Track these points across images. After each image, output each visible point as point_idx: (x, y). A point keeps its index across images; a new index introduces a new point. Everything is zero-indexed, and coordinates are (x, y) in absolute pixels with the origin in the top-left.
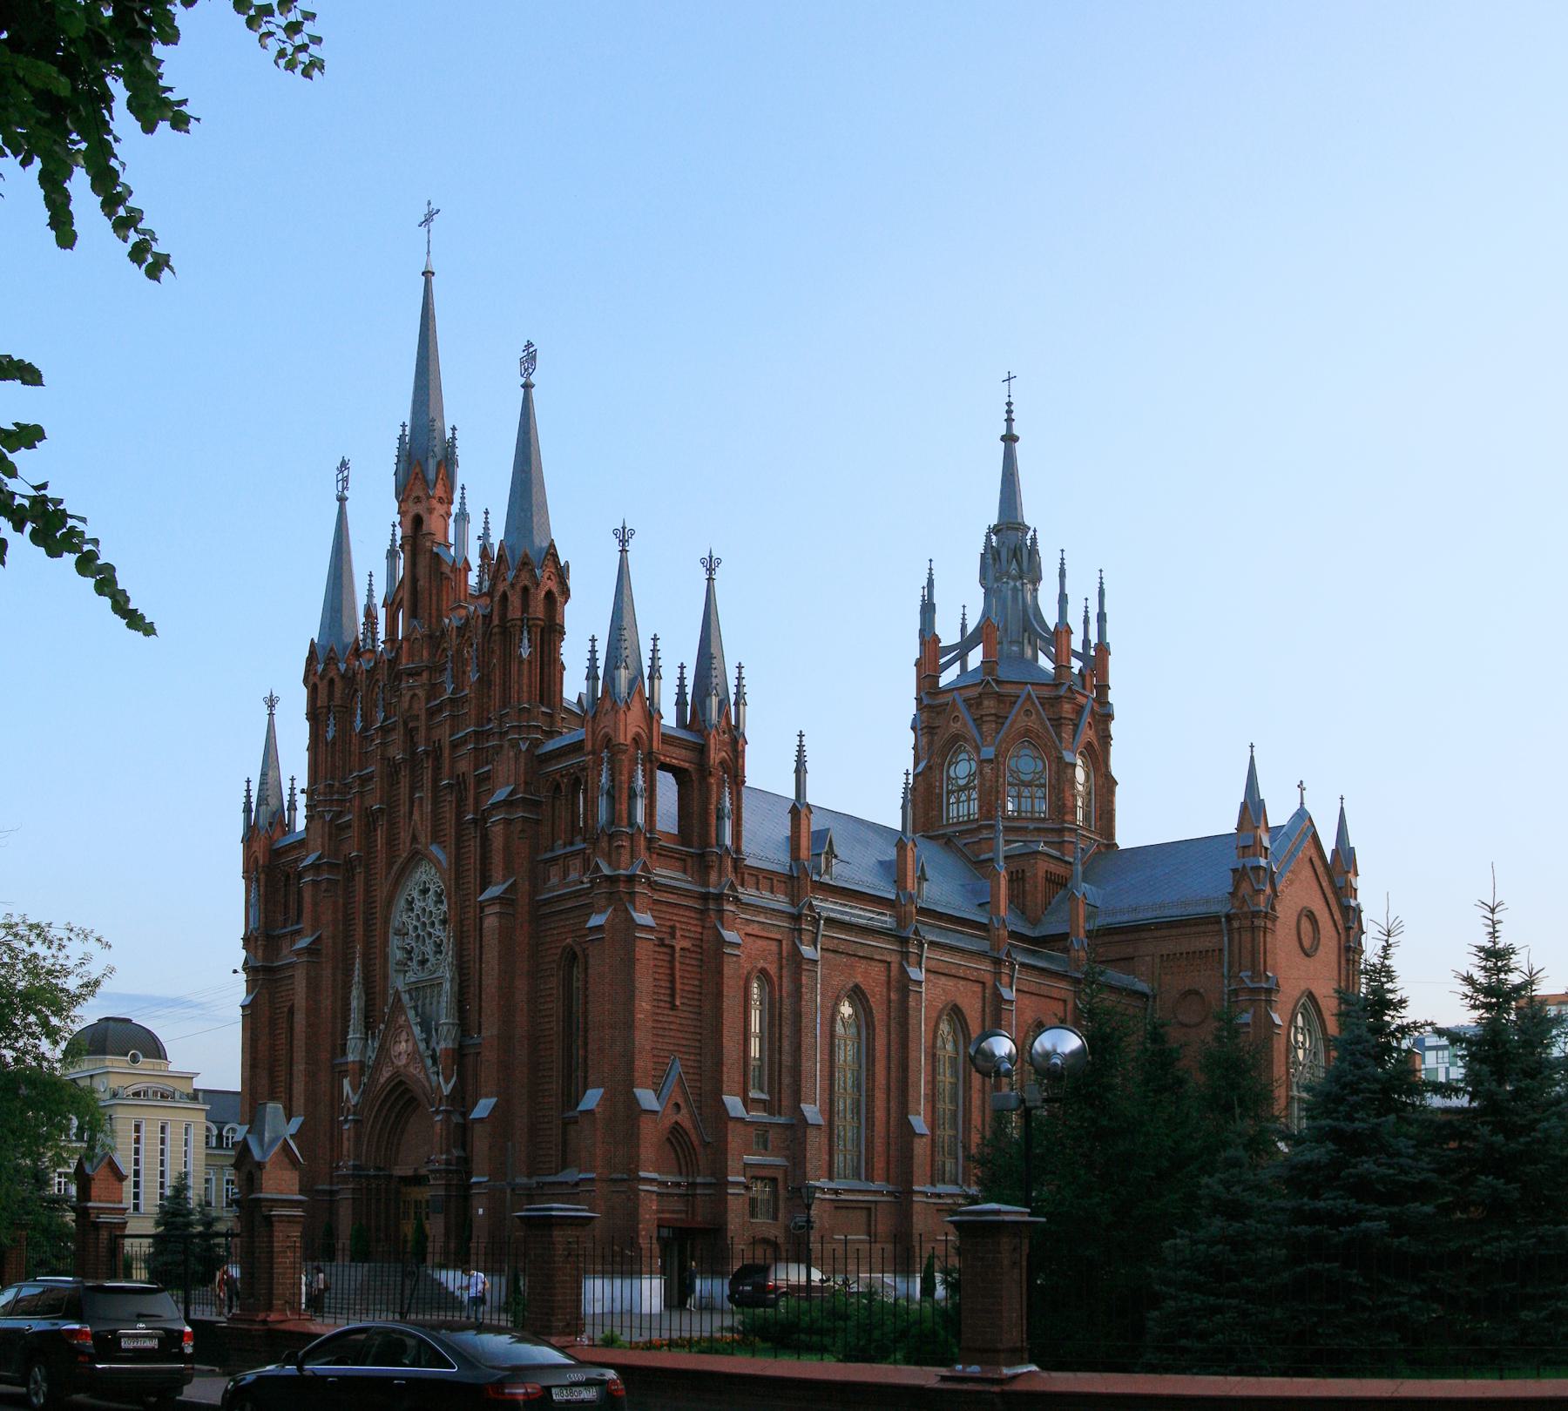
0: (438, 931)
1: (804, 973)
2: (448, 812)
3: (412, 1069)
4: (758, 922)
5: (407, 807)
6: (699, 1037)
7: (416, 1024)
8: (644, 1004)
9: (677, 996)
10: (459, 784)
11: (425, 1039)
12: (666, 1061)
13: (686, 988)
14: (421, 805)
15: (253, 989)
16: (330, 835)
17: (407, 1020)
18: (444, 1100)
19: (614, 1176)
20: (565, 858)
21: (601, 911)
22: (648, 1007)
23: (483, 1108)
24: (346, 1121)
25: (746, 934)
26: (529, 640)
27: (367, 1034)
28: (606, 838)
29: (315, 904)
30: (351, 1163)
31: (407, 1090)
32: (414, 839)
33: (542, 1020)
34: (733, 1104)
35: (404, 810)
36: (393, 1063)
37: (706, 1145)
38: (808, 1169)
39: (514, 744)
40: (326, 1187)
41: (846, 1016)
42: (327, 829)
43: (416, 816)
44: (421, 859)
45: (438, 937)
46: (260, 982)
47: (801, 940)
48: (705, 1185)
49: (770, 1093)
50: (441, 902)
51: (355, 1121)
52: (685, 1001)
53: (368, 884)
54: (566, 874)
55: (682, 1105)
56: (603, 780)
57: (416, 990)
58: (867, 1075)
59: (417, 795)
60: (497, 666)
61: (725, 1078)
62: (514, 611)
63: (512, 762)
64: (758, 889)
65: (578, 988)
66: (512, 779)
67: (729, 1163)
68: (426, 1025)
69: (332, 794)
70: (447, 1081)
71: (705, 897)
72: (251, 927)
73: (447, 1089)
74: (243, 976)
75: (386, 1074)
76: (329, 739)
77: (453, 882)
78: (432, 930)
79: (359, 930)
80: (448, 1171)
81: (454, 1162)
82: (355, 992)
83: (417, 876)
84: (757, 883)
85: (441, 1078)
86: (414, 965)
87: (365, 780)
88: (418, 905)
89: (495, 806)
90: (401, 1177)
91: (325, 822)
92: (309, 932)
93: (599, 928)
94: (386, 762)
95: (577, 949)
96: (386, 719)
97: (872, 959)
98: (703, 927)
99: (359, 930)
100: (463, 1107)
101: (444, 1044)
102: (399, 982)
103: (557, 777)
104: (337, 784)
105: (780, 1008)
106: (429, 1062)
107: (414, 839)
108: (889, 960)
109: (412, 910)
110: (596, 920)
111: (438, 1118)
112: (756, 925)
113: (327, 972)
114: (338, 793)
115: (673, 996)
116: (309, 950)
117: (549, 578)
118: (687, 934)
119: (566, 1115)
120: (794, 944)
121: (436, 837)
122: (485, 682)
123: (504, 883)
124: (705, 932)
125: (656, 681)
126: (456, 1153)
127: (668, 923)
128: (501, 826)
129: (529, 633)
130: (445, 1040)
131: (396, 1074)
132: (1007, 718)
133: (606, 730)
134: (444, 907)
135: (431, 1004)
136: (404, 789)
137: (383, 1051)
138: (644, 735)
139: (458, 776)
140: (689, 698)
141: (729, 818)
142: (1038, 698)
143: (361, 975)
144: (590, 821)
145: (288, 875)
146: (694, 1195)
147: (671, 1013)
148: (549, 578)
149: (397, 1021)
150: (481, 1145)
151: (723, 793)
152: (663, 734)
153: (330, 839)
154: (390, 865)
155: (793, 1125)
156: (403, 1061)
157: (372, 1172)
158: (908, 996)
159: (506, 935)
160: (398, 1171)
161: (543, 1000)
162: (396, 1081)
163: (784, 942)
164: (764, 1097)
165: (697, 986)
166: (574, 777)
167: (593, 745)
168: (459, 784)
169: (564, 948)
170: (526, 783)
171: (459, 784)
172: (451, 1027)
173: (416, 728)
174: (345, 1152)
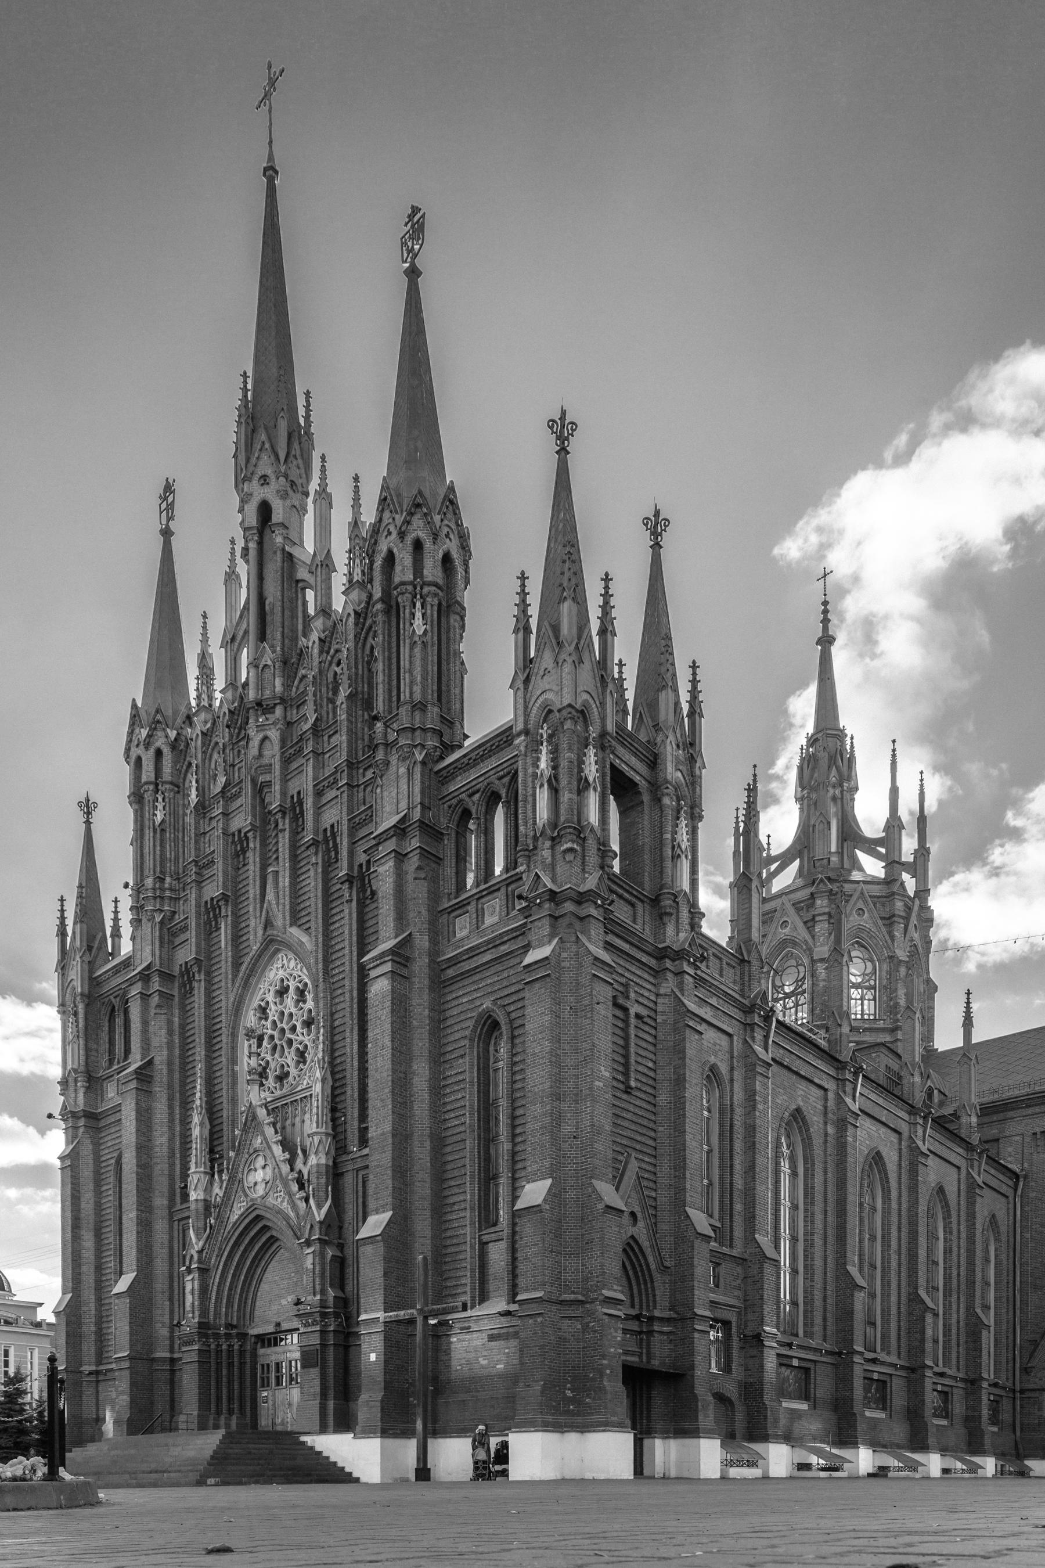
1: (759, 1078)
2: (312, 882)
5: (258, 887)
8: (602, 1068)
19: (566, 1297)
20: (478, 899)
32: (268, 924)
35: (253, 891)
38: (765, 1313)
43: (270, 896)
67: (696, 1292)
89: (381, 839)
97: (811, 1082)
107: (268, 924)
121: (295, 919)
123: (396, 937)
158: (846, 1130)
159: (400, 1004)
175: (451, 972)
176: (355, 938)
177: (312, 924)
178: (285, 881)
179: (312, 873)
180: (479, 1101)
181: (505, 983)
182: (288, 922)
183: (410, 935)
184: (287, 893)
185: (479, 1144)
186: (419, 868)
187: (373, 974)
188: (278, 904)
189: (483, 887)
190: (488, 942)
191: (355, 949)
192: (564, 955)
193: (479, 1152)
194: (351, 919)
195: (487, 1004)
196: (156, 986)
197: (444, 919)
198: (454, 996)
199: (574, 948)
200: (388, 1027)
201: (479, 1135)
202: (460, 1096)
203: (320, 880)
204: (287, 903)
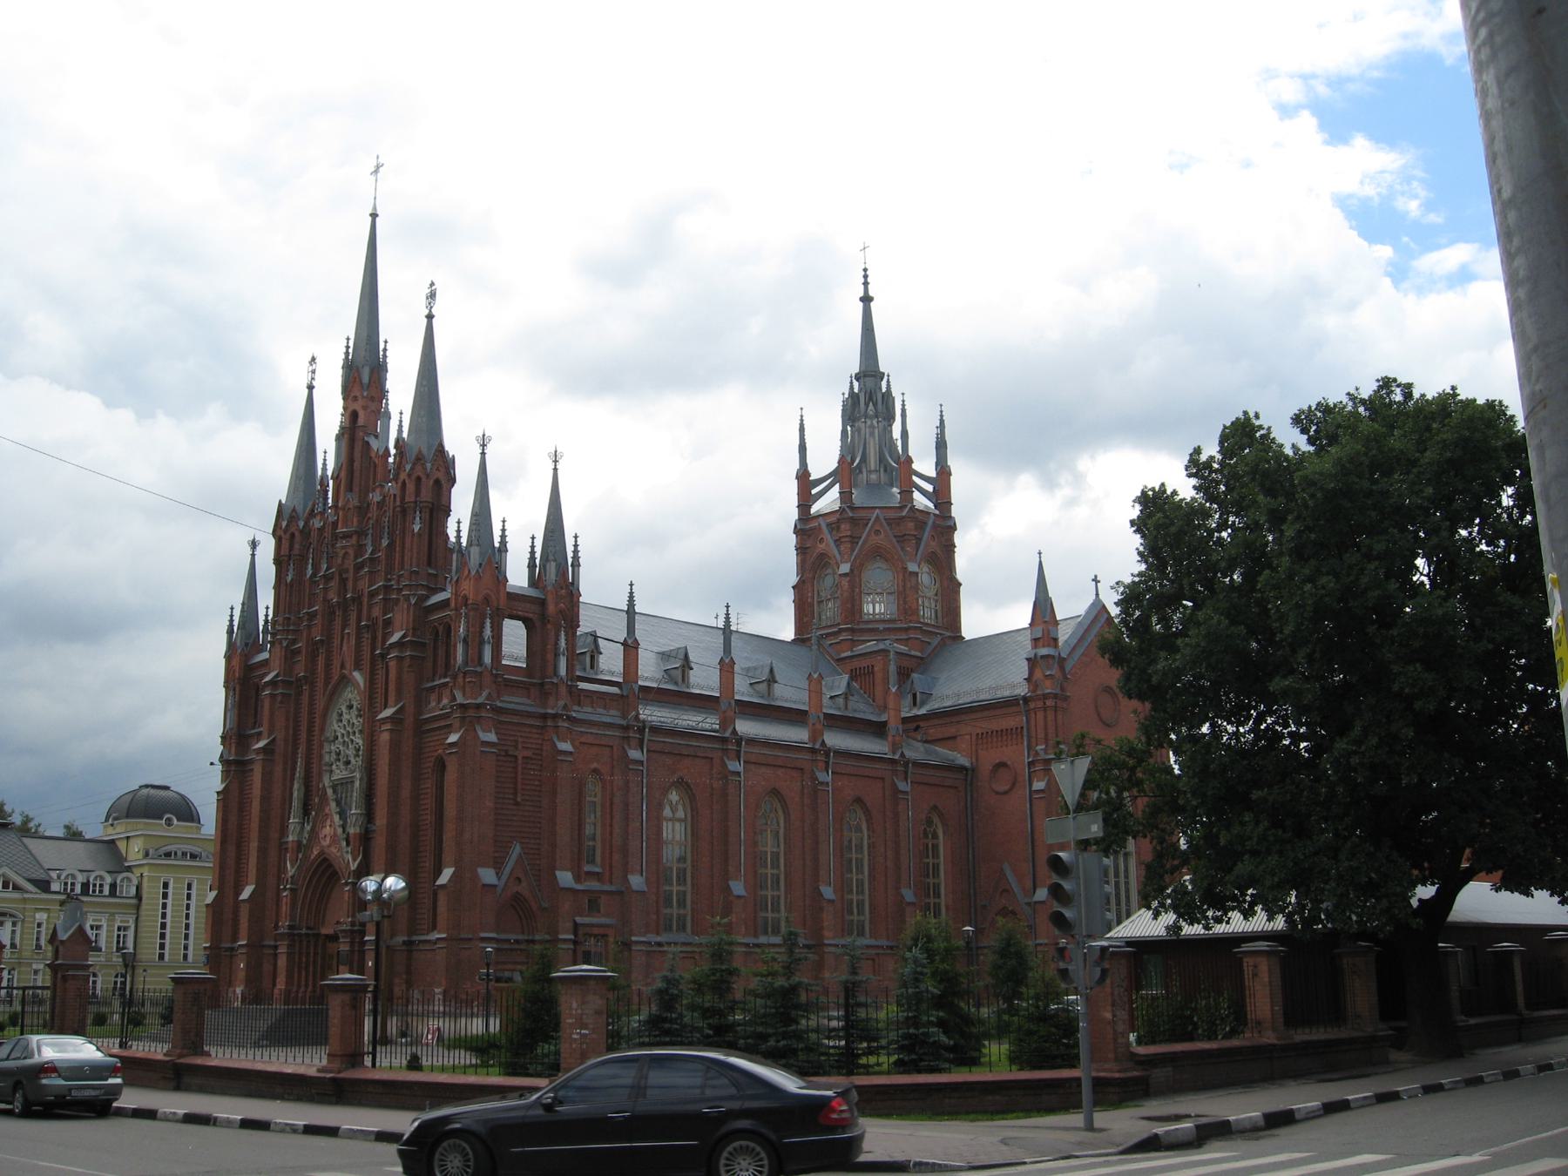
3: (334, 850)
4: (591, 733)
7: (336, 813)
9: (519, 795)
14: (348, 639)
15: (227, 778)
16: (286, 658)
18: (352, 874)
24: (285, 889)
25: (581, 743)
26: (420, 518)
27: (304, 819)
28: (462, 674)
29: (272, 714)
30: (287, 924)
31: (330, 866)
32: (343, 666)
34: (565, 878)
35: (336, 642)
39: (407, 598)
41: (674, 803)
42: (283, 654)
43: (345, 648)
46: (232, 772)
51: (291, 889)
52: (527, 798)
54: (439, 701)
56: (461, 630)
59: (347, 631)
62: (410, 498)
63: (405, 612)
64: (593, 707)
68: (342, 814)
69: (288, 625)
70: (354, 860)
71: (545, 717)
72: (227, 727)
74: (219, 767)
76: (288, 581)
78: (353, 738)
79: (303, 736)
80: (352, 932)
82: (296, 786)
83: (346, 694)
84: (592, 703)
87: (312, 616)
88: (346, 717)
90: (327, 936)
91: (282, 647)
92: (267, 736)
96: (326, 570)
99: (303, 736)
102: (326, 781)
104: (292, 618)
108: (710, 756)
109: (341, 721)
110: (453, 738)
112: (589, 735)
113: (278, 769)
115: (515, 794)
116: (264, 750)
120: (623, 748)
121: (358, 666)
122: (391, 545)
123: (395, 706)
125: (503, 554)
127: (512, 738)
129: (420, 513)
131: (322, 853)
132: (861, 537)
136: (338, 622)
137: (314, 833)
138: (493, 597)
140: (538, 561)
141: (564, 655)
142: (885, 519)
143: (303, 770)
149: (324, 810)
151: (560, 635)
152: (508, 593)
153: (285, 663)
154: (327, 683)
157: (304, 931)
159: (395, 746)
160: (324, 931)
162: (322, 858)
163: (615, 748)
164: (597, 870)
165: (537, 786)
167: (456, 604)
169: (437, 758)
170: (414, 629)
171: (372, 627)
173: (347, 579)
186: (409, 666)
196: (280, 691)
200: (387, 761)
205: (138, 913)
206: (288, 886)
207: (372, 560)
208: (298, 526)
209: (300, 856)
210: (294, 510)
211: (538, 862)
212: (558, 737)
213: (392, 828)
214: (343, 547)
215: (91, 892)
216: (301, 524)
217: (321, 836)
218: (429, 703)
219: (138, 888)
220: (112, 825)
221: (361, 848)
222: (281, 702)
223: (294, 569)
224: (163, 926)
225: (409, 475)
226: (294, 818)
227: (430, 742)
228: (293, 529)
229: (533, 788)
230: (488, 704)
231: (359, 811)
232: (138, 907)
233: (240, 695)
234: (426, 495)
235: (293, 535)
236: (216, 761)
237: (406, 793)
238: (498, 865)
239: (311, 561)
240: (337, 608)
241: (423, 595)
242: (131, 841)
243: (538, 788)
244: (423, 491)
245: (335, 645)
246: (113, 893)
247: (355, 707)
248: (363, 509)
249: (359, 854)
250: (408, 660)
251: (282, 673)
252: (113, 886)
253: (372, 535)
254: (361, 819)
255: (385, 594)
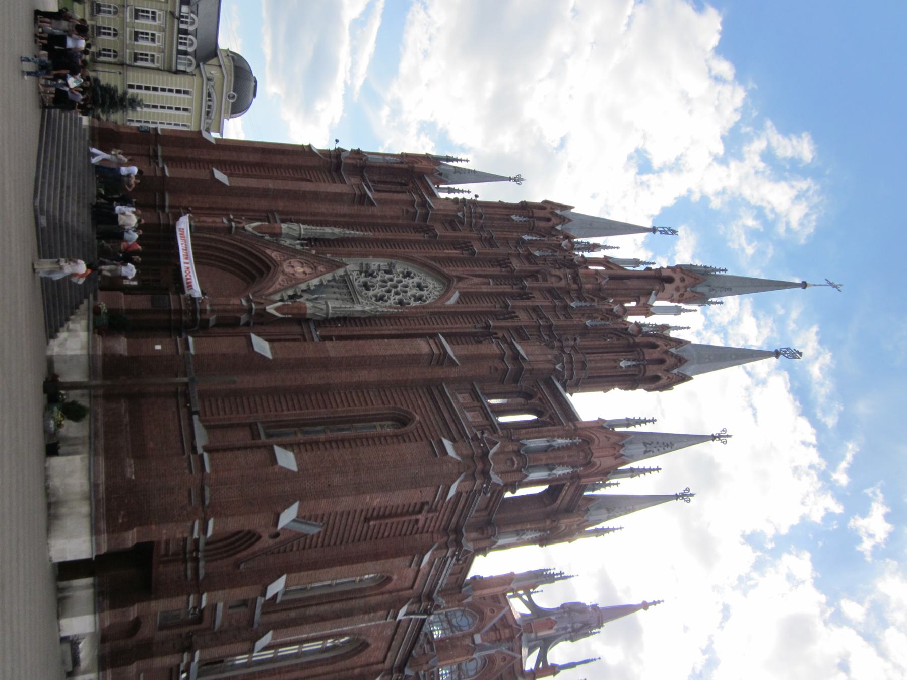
0: (393, 299)
2: (485, 305)
3: (281, 278)
5: (480, 273)
6: (338, 542)
7: (321, 281)
9: (378, 522)
10: (509, 313)
11: (309, 289)
12: (319, 520)
13: (383, 527)
14: (484, 284)
16: (446, 215)
17: (322, 274)
18: (260, 307)
20: (481, 407)
21: (456, 450)
22: (375, 504)
23: (261, 346)
24: (230, 220)
27: (304, 239)
28: (516, 448)
29: (396, 202)
31: (261, 274)
32: (460, 279)
33: (342, 395)
35: (478, 270)
36: (285, 260)
37: (237, 565)
39: (558, 359)
40: (167, 203)
43: (476, 280)
44: (444, 284)
45: (389, 298)
46: (329, 160)
47: (413, 603)
48: (196, 570)
49: (282, 602)
50: (415, 301)
53: (418, 242)
54: (470, 409)
55: (277, 540)
57: (345, 281)
58: (292, 666)
60: (602, 342)
61: (302, 573)
65: (375, 427)
66: (531, 358)
69: (475, 217)
70: (277, 309)
71: (458, 531)
73: (270, 309)
75: (274, 255)
77: (436, 310)
79: (382, 235)
80: (194, 312)
81: (205, 317)
82: (337, 230)
83: (430, 281)
85: (280, 304)
86: (363, 279)
88: (407, 281)
93: (444, 452)
94: (506, 257)
95: (411, 427)
98: (432, 533)
99: (382, 235)
100: (254, 324)
101: (310, 307)
102: (352, 267)
103: (539, 395)
104: (482, 221)
105: (356, 598)
106: (291, 292)
107: (460, 279)
109: (404, 277)
111: (244, 302)
113: (345, 209)
114: (476, 223)
115: (378, 517)
117: (668, 378)
118: (428, 521)
119: (259, 425)
120: (409, 599)
121: (464, 296)
122: (585, 331)
123: (455, 355)
124: (429, 535)
126: (212, 319)
128: (498, 352)
129: (634, 365)
130: (314, 307)
131: (277, 265)
133: (596, 439)
134: (413, 304)
135: (334, 293)
137: (292, 253)
139: (514, 313)
143: (350, 236)
144: (523, 431)
145: (406, 185)
146: (185, 561)
147: (362, 518)
148: (668, 378)
149: (320, 264)
150: (224, 345)
154: (434, 259)
155: (252, 625)
156: (288, 270)
159: (414, 359)
161: (360, 395)
165: (384, 534)
166: (542, 409)
168: (510, 315)
169: (410, 413)
172: (325, 312)
173: (537, 280)
174: (201, 219)
175: (436, 393)
176: (454, 331)
177: (461, 305)
178: (485, 289)
179: (490, 304)
180: (354, 416)
181: (431, 429)
182: (461, 290)
183: (457, 365)
184: (478, 290)
185: (323, 418)
187: (431, 342)
188: (471, 284)
189: (489, 410)
190: (456, 415)
191: (448, 331)
192: (450, 466)
193: (318, 418)
194: (466, 328)
195: (418, 418)
197: (468, 386)
198: (422, 395)
199: (456, 471)
201: (330, 418)
202: (356, 403)
203: (487, 309)
204: (472, 290)
205: (164, 70)
206: (233, 224)
207: (566, 307)
208: (557, 225)
209: (267, 237)
210: (570, 220)
211: (295, 548)
212: (436, 549)
213: (326, 364)
214: (565, 275)
215: (180, 36)
216: (559, 227)
217: (292, 261)
218: (459, 394)
219: (184, 72)
220: (228, 55)
221: (290, 316)
222: (407, 211)
223: (520, 221)
224: (155, 89)
225: (666, 352)
226: (304, 229)
227: (421, 397)
228: (554, 220)
229: (382, 531)
230: (487, 486)
231: (330, 311)
232: (170, 71)
233: (399, 168)
234: (652, 370)
235: (549, 220)
236: (338, 145)
237: (364, 375)
238: (301, 518)
239: (534, 238)
240: (509, 269)
241: (564, 376)
242: (218, 69)
243: (380, 535)
244: (655, 367)
245: (476, 269)
246: (180, 52)
247: (422, 293)
248: (599, 293)
249: (282, 314)
250: (502, 367)
251: (435, 212)
252: (185, 53)
253: (585, 306)
254: (322, 314)
255: (544, 327)
